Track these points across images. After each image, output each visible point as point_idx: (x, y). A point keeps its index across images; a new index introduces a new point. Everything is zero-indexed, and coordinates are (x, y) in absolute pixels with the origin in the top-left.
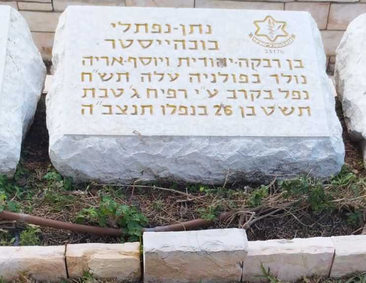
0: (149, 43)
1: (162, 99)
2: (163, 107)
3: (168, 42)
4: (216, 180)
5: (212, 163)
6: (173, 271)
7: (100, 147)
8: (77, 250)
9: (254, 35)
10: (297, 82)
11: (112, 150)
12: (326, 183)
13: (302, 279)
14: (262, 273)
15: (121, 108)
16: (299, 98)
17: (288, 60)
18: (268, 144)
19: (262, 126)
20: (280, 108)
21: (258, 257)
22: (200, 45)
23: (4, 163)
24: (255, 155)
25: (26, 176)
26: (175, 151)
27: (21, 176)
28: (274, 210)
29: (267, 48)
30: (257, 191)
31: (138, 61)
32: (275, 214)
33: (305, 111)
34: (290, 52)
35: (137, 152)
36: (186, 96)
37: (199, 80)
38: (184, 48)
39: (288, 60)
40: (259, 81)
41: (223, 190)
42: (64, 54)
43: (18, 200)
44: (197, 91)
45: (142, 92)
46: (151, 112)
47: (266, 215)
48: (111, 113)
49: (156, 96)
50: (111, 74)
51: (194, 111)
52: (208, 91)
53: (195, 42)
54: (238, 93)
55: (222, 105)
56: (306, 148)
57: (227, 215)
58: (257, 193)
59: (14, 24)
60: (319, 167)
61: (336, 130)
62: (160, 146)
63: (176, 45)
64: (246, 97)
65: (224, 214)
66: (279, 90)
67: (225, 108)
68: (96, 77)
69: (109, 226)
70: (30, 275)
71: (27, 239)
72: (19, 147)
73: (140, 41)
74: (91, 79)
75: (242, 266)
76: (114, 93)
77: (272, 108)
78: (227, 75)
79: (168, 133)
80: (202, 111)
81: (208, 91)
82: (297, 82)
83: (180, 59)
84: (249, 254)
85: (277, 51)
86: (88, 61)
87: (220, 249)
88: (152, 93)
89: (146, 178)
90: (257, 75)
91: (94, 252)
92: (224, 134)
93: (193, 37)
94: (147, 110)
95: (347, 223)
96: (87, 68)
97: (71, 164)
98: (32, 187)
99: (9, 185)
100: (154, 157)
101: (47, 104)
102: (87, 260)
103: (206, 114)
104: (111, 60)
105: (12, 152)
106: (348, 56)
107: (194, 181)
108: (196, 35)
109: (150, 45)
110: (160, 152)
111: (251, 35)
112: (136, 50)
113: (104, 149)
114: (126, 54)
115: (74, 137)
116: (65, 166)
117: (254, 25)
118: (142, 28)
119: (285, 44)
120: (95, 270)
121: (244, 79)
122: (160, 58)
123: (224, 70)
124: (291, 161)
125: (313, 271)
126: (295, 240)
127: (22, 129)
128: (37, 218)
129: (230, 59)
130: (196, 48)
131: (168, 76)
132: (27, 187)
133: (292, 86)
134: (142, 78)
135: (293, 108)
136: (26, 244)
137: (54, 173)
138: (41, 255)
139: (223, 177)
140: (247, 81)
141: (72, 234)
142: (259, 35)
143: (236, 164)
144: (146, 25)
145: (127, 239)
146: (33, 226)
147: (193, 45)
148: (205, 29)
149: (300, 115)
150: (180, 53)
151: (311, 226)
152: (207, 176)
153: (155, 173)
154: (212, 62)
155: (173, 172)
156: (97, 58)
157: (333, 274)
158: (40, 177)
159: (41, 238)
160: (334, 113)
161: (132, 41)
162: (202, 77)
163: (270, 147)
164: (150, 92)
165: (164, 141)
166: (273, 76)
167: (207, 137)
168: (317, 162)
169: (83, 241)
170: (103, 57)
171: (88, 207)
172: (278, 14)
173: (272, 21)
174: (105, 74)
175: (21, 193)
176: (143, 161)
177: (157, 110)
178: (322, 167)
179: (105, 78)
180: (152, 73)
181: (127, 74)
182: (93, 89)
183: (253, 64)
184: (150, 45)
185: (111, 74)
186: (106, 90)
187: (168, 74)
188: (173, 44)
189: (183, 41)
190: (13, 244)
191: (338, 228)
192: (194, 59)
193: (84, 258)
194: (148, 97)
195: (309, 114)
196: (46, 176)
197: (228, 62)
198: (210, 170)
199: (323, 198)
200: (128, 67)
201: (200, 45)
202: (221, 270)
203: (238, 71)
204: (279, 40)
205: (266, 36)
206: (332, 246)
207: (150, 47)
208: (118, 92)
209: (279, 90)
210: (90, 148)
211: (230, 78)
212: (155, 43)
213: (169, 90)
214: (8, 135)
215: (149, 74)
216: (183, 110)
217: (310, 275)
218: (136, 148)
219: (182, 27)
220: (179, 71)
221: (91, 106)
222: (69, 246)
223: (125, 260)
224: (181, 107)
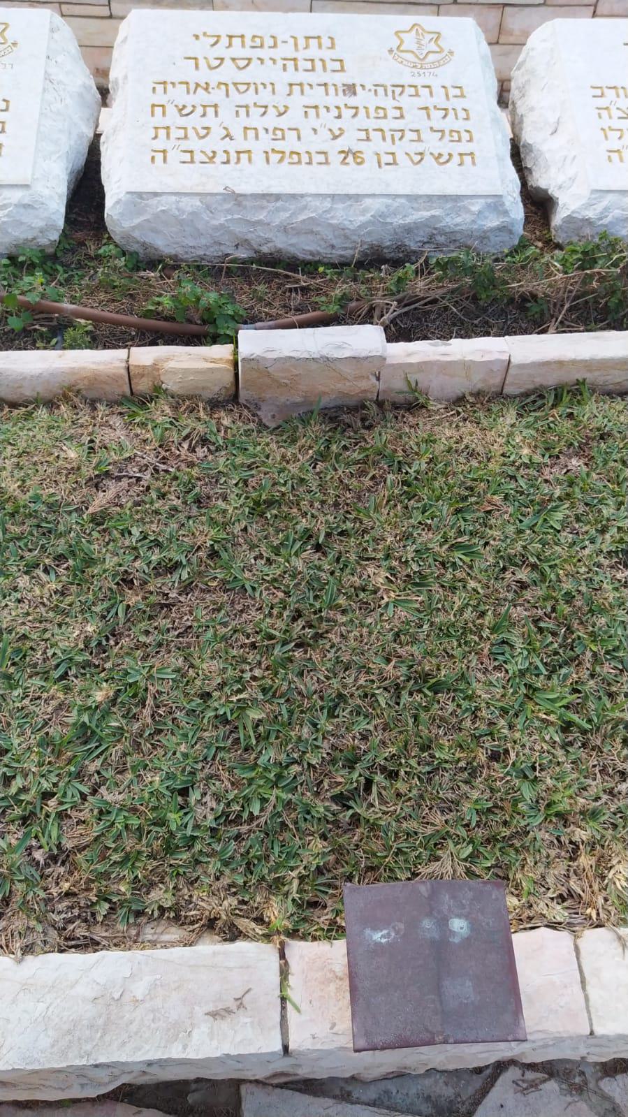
0: (246, 62)
1: (266, 142)
2: (266, 153)
3: (274, 61)
4: (342, 256)
5: (336, 233)
6: (280, 385)
7: (178, 209)
8: (144, 356)
9: (395, 51)
10: (457, 118)
11: (194, 214)
12: (497, 260)
13: (464, 397)
14: (406, 389)
15: (206, 155)
16: (459, 141)
17: (444, 87)
18: (415, 205)
19: (405, 180)
20: (431, 154)
21: (400, 366)
22: (319, 65)
23: (41, 232)
24: (398, 221)
25: (73, 251)
26: (284, 216)
27: (65, 251)
28: (423, 298)
29: (414, 70)
30: (400, 272)
31: (231, 87)
32: (426, 304)
33: (468, 159)
34: (446, 75)
35: (229, 217)
36: (299, 138)
37: (318, 115)
38: (296, 69)
39: (444, 87)
40: (402, 117)
41: (352, 271)
42: (126, 77)
43: (61, 284)
44: (315, 130)
45: (237, 132)
46: (250, 160)
47: (413, 306)
48: (192, 161)
49: (257, 137)
50: (193, 106)
51: (310, 158)
52: (330, 130)
53: (312, 60)
54: (372, 134)
55: (350, 150)
56: (469, 211)
57: (357, 307)
58: (400, 275)
59: (56, 36)
60: (488, 238)
61: (511, 185)
62: (263, 208)
63: (284, 65)
64: (384, 139)
65: (353, 304)
66: (431, 128)
67: (354, 154)
68: (171, 110)
69: (190, 321)
70: (78, 391)
71: (74, 340)
72: (63, 210)
73: (233, 59)
74: (164, 114)
75: (378, 379)
76: (197, 134)
77: (421, 154)
78: (357, 108)
79: (275, 190)
80: (322, 158)
81: (330, 130)
82: (457, 118)
83: (291, 85)
84: (389, 361)
85: (427, 74)
86: (160, 88)
87: (347, 354)
88: (251, 134)
89: (243, 254)
90: (400, 108)
91: (168, 359)
92: (352, 191)
93: (309, 53)
94: (244, 157)
95: (526, 317)
96: (160, 98)
97: (136, 234)
98: (80, 266)
99: (49, 264)
100: (254, 224)
101: (102, 148)
102: (158, 370)
103: (327, 163)
104: (192, 87)
105: (54, 217)
106: (529, 81)
107: (310, 257)
108: (314, 52)
109: (248, 65)
110: (261, 217)
111: (391, 51)
112: (228, 73)
113: (183, 212)
114: (214, 77)
115: (140, 195)
116: (127, 237)
117: (395, 37)
118: (237, 41)
119: (439, 64)
120: (170, 384)
121: (381, 113)
122: (263, 84)
123: (352, 101)
124: (448, 230)
125: (480, 386)
126: (453, 341)
127: (66, 184)
128: (88, 310)
129: (362, 85)
130: (313, 70)
131: (274, 109)
132: (73, 266)
133: (450, 123)
134: (237, 112)
135: (450, 155)
136: (72, 347)
137: (112, 247)
138: (94, 363)
139: (351, 252)
140: (385, 117)
141: (137, 333)
142: (402, 51)
143: (369, 233)
144: (242, 37)
145: (215, 339)
146: (83, 321)
147: (308, 65)
148: (326, 42)
149: (460, 165)
150: (291, 76)
151: (476, 322)
152: (329, 251)
153: (255, 247)
154: (336, 90)
155: (280, 245)
156: (173, 84)
157: (507, 390)
158: (92, 253)
159: (94, 339)
160: (509, 162)
161: (222, 59)
162: (322, 111)
163: (418, 210)
164: (248, 131)
165: (268, 201)
166: (422, 109)
167: (329, 196)
168: (485, 232)
169: (153, 343)
170: (181, 83)
171: (160, 295)
172: (429, 21)
173: (420, 31)
174: (184, 107)
175: (66, 275)
176: (239, 229)
177: (259, 158)
178: (492, 238)
179: (184, 112)
180: (251, 105)
181: (216, 106)
182: (168, 128)
183: (393, 92)
184: (248, 65)
185: (193, 106)
186: (185, 129)
187: (274, 106)
188: (280, 63)
189: (295, 59)
190: (54, 348)
191: (514, 325)
192: (310, 85)
193: (155, 367)
194: (246, 138)
195: (474, 163)
196: (101, 251)
197: (359, 89)
198: (334, 242)
199: (493, 283)
200: (217, 96)
201: (319, 65)
202: (348, 384)
203: (372, 102)
204: (431, 57)
205: (412, 52)
206: (507, 349)
207: (249, 68)
208: (203, 132)
209: (431, 128)
210: (163, 211)
211: (362, 112)
212: (255, 62)
213: (275, 129)
214: (46, 192)
215: (247, 107)
216: (295, 158)
217: (475, 390)
218: (228, 211)
219: (293, 40)
220: (289, 101)
221: (164, 152)
222: (133, 349)
223: (212, 370)
224: (292, 153)
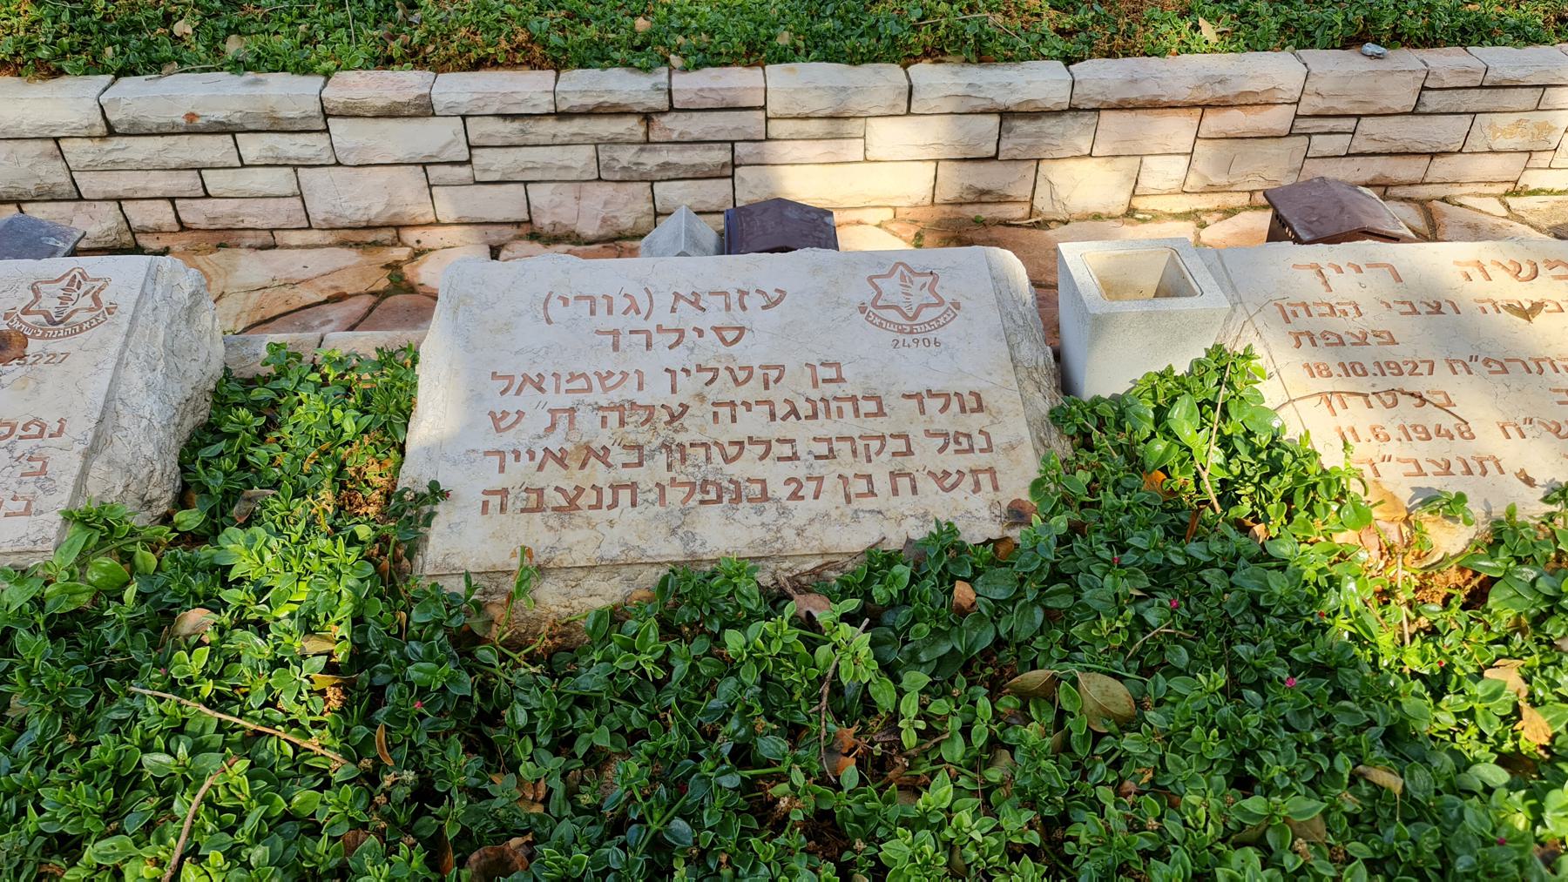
64: (854, 452)
94: (625, 496)
166: (909, 397)
204: (927, 314)
205: (897, 308)
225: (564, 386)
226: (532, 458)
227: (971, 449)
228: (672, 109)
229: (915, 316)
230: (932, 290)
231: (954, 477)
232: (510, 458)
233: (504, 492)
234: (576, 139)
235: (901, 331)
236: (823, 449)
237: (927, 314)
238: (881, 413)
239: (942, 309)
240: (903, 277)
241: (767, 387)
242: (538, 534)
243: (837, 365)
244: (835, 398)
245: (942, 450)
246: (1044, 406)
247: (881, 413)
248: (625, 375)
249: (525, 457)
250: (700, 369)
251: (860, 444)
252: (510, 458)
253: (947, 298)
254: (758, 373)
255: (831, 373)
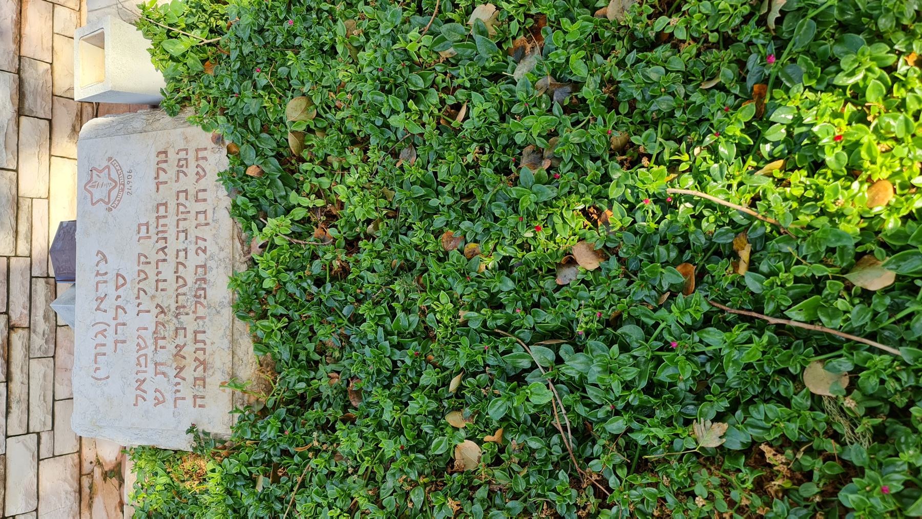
94: (200, 337)
166: (158, 189)
204: (114, 175)
225: (143, 368)
226: (179, 384)
227: (186, 159)
228: (7, 313)
229: (115, 182)
230: (101, 171)
231: (199, 169)
232: (178, 395)
233: (195, 397)
234: (25, 370)
235: (123, 190)
236: (182, 235)
237: (114, 175)
238: (165, 204)
239: (112, 167)
240: (93, 186)
241: (149, 263)
242: (216, 378)
243: (139, 225)
244: (157, 227)
245: (186, 175)
246: (168, 118)
247: (165, 204)
248: (139, 337)
249: (178, 387)
250: (138, 298)
251: (181, 216)
252: (178, 395)
253: (106, 163)
254: (142, 267)
255: (144, 229)
